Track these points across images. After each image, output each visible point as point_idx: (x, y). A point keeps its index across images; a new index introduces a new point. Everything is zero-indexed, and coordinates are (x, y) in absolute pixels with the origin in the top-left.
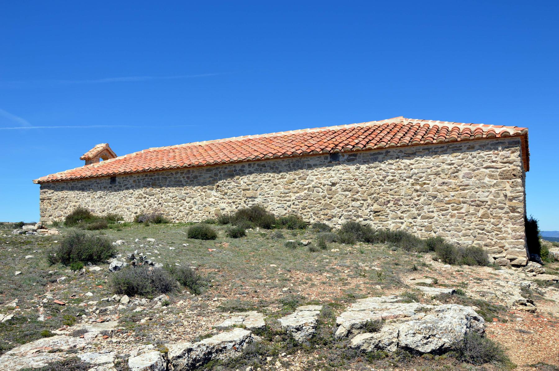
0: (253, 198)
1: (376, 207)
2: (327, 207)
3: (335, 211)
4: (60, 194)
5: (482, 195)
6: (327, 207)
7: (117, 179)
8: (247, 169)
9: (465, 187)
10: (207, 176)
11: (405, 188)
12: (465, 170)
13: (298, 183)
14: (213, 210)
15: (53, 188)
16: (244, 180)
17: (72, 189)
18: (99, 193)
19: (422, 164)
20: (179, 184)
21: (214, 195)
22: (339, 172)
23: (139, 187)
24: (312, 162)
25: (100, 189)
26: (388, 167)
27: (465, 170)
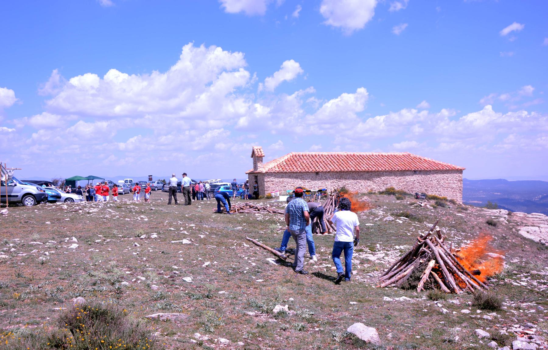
0: (387, 184)
1: (426, 188)
3: (414, 189)
5: (454, 186)
6: (412, 188)
7: (320, 174)
8: (385, 173)
9: (449, 183)
10: (367, 175)
11: (435, 182)
12: (450, 179)
14: (369, 188)
17: (290, 177)
19: (439, 176)
21: (369, 183)
24: (408, 173)
26: (431, 177)
27: (450, 179)
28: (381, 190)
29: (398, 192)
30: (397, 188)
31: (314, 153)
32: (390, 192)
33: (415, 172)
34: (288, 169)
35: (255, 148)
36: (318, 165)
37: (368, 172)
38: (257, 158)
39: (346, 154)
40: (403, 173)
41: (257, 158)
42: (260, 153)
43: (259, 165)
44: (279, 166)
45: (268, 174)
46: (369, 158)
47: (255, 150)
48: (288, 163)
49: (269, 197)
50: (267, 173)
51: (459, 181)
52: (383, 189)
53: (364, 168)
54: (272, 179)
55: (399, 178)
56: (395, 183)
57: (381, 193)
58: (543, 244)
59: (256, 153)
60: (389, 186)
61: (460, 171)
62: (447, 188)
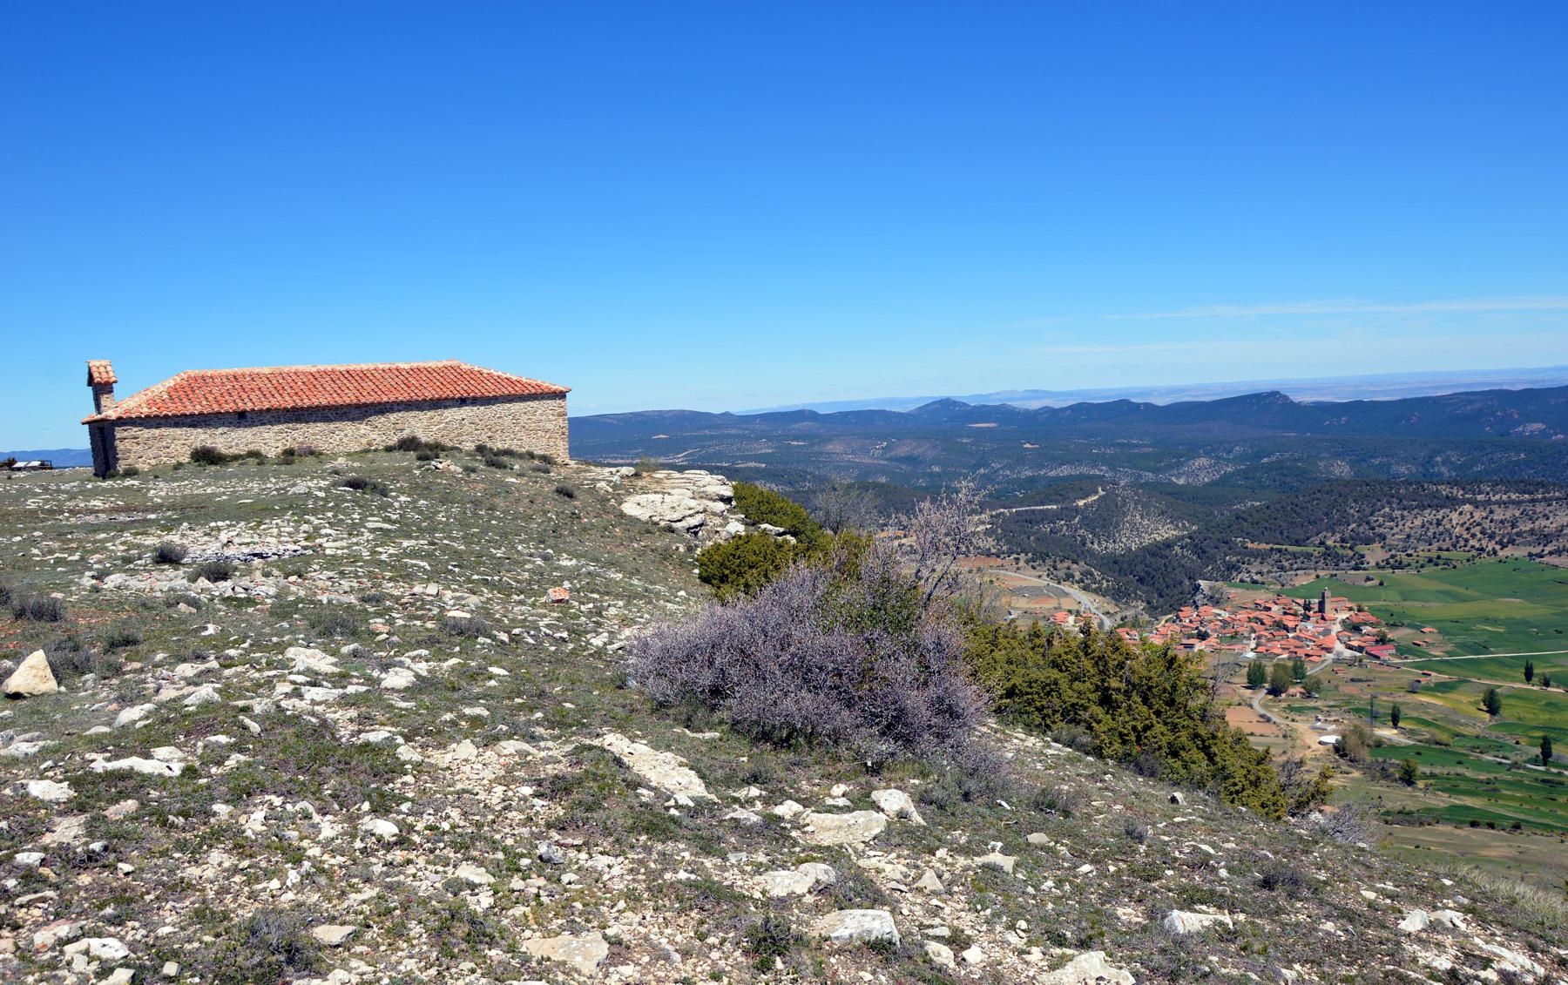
2: (460, 435)
4: (157, 432)
5: (549, 426)
6: (460, 435)
11: (508, 421)
13: (437, 419)
14: (364, 441)
15: (140, 425)
16: (393, 417)
17: (177, 425)
18: (220, 430)
19: (516, 407)
20: (327, 420)
21: (363, 428)
22: (466, 412)
23: (279, 422)
25: (223, 425)
28: (391, 443)
29: (427, 445)
30: (424, 438)
31: (238, 370)
32: (409, 444)
33: (462, 402)
34: (173, 409)
35: (94, 363)
36: (244, 396)
37: (358, 406)
38: (101, 388)
39: (314, 370)
40: (437, 404)
41: (101, 388)
42: (104, 375)
43: (104, 400)
44: (151, 403)
45: (122, 422)
46: (363, 375)
47: (94, 369)
48: (175, 395)
49: (131, 473)
50: (120, 418)
51: (560, 415)
52: (394, 440)
53: (349, 397)
54: (134, 431)
55: (430, 414)
56: (421, 426)
57: (389, 449)
58: (657, 524)
59: (96, 375)
60: (406, 434)
61: (561, 395)
62: (534, 431)
